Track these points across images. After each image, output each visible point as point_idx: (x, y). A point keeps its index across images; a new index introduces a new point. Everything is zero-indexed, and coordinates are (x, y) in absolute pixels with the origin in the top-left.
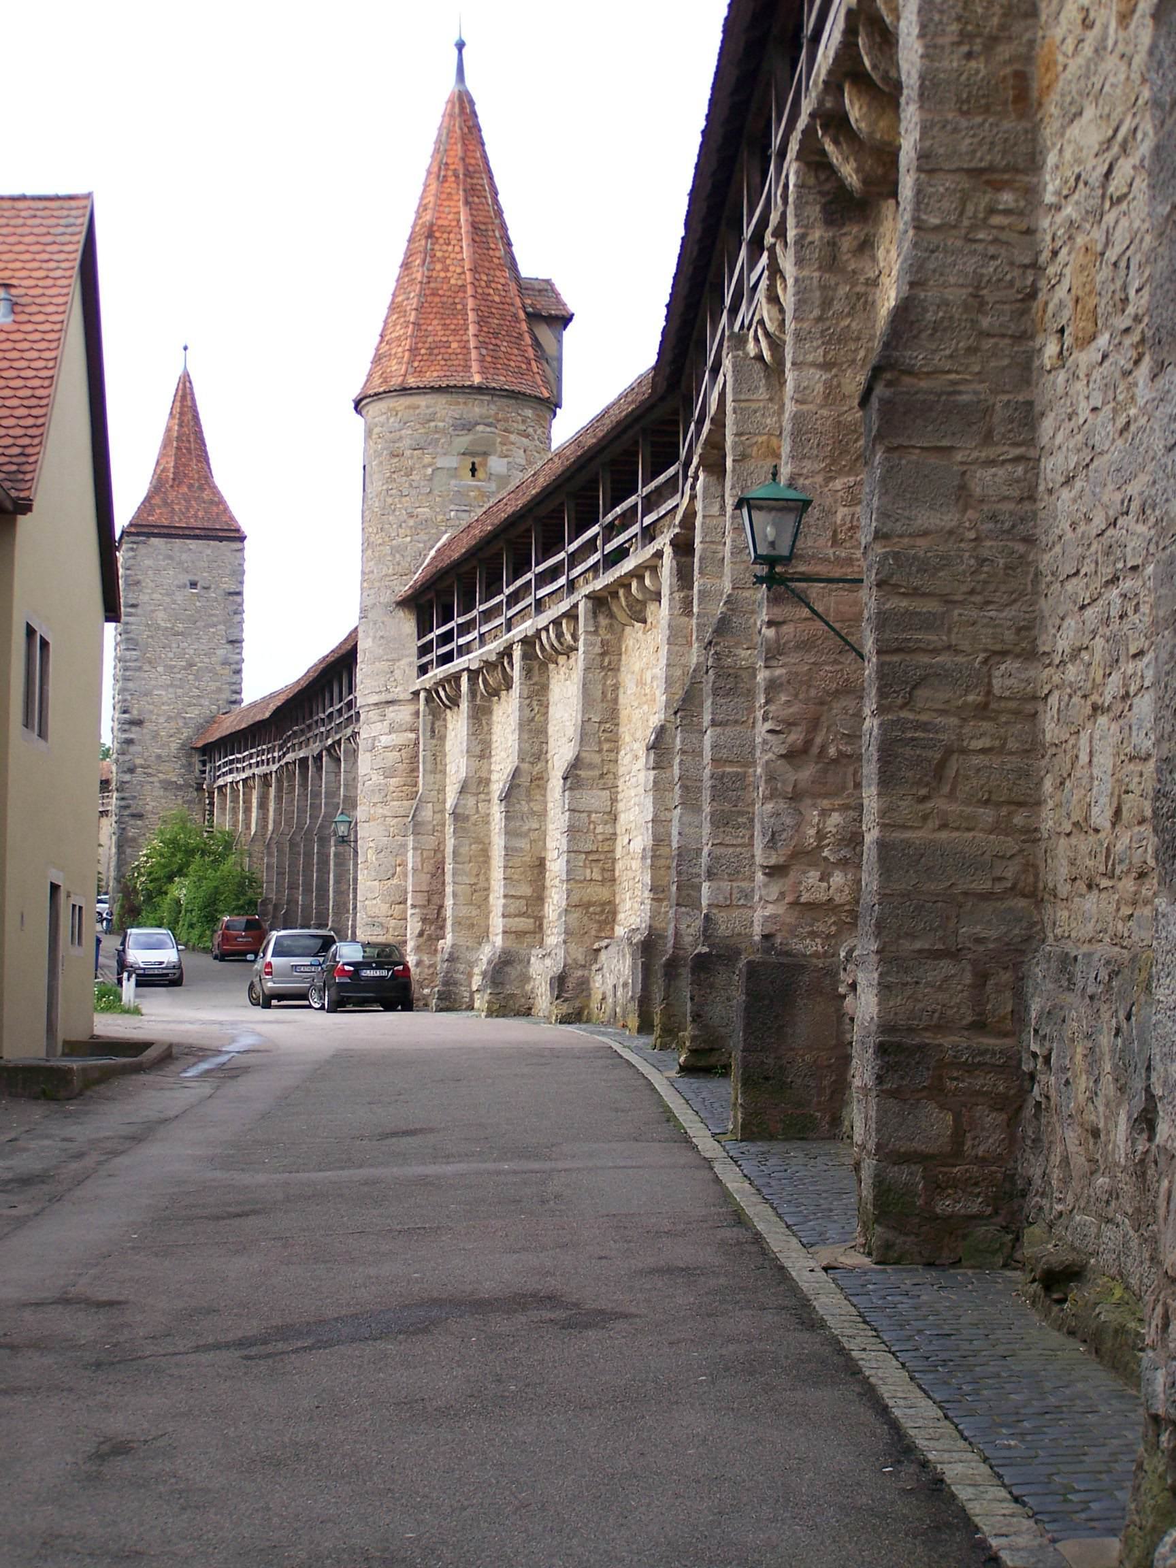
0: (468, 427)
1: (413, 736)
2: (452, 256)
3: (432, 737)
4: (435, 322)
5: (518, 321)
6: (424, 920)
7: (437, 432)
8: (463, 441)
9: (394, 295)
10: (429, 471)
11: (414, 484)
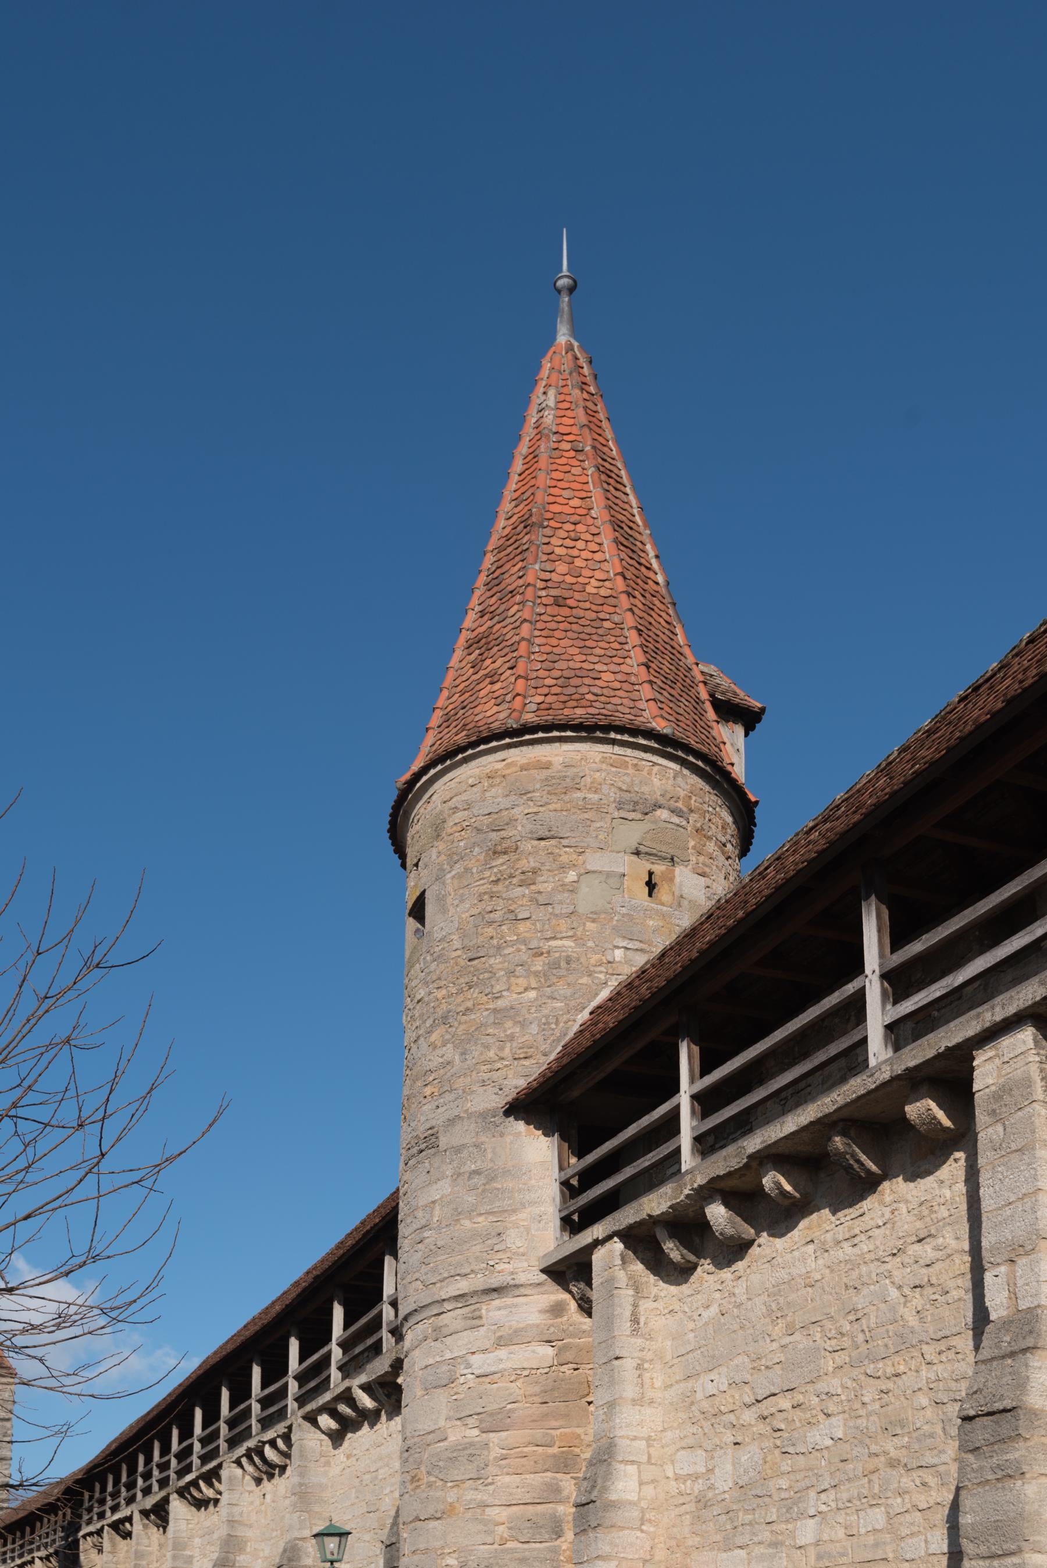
2: (585, 555)
3: (635, 1332)
4: (565, 643)
7: (584, 809)
10: (572, 876)
11: (542, 899)
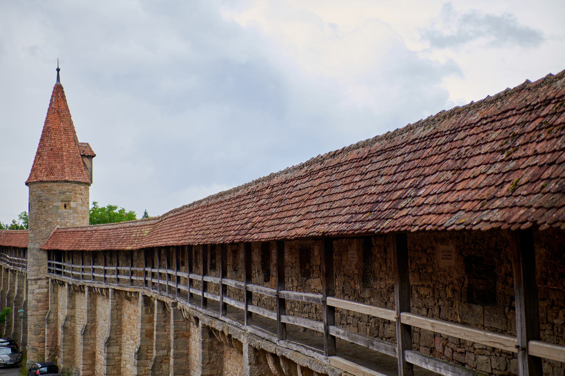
0: (64, 193)
1: (46, 290)
3: (54, 292)
5: (79, 158)
6: (51, 350)
8: (62, 197)
9: (38, 149)
